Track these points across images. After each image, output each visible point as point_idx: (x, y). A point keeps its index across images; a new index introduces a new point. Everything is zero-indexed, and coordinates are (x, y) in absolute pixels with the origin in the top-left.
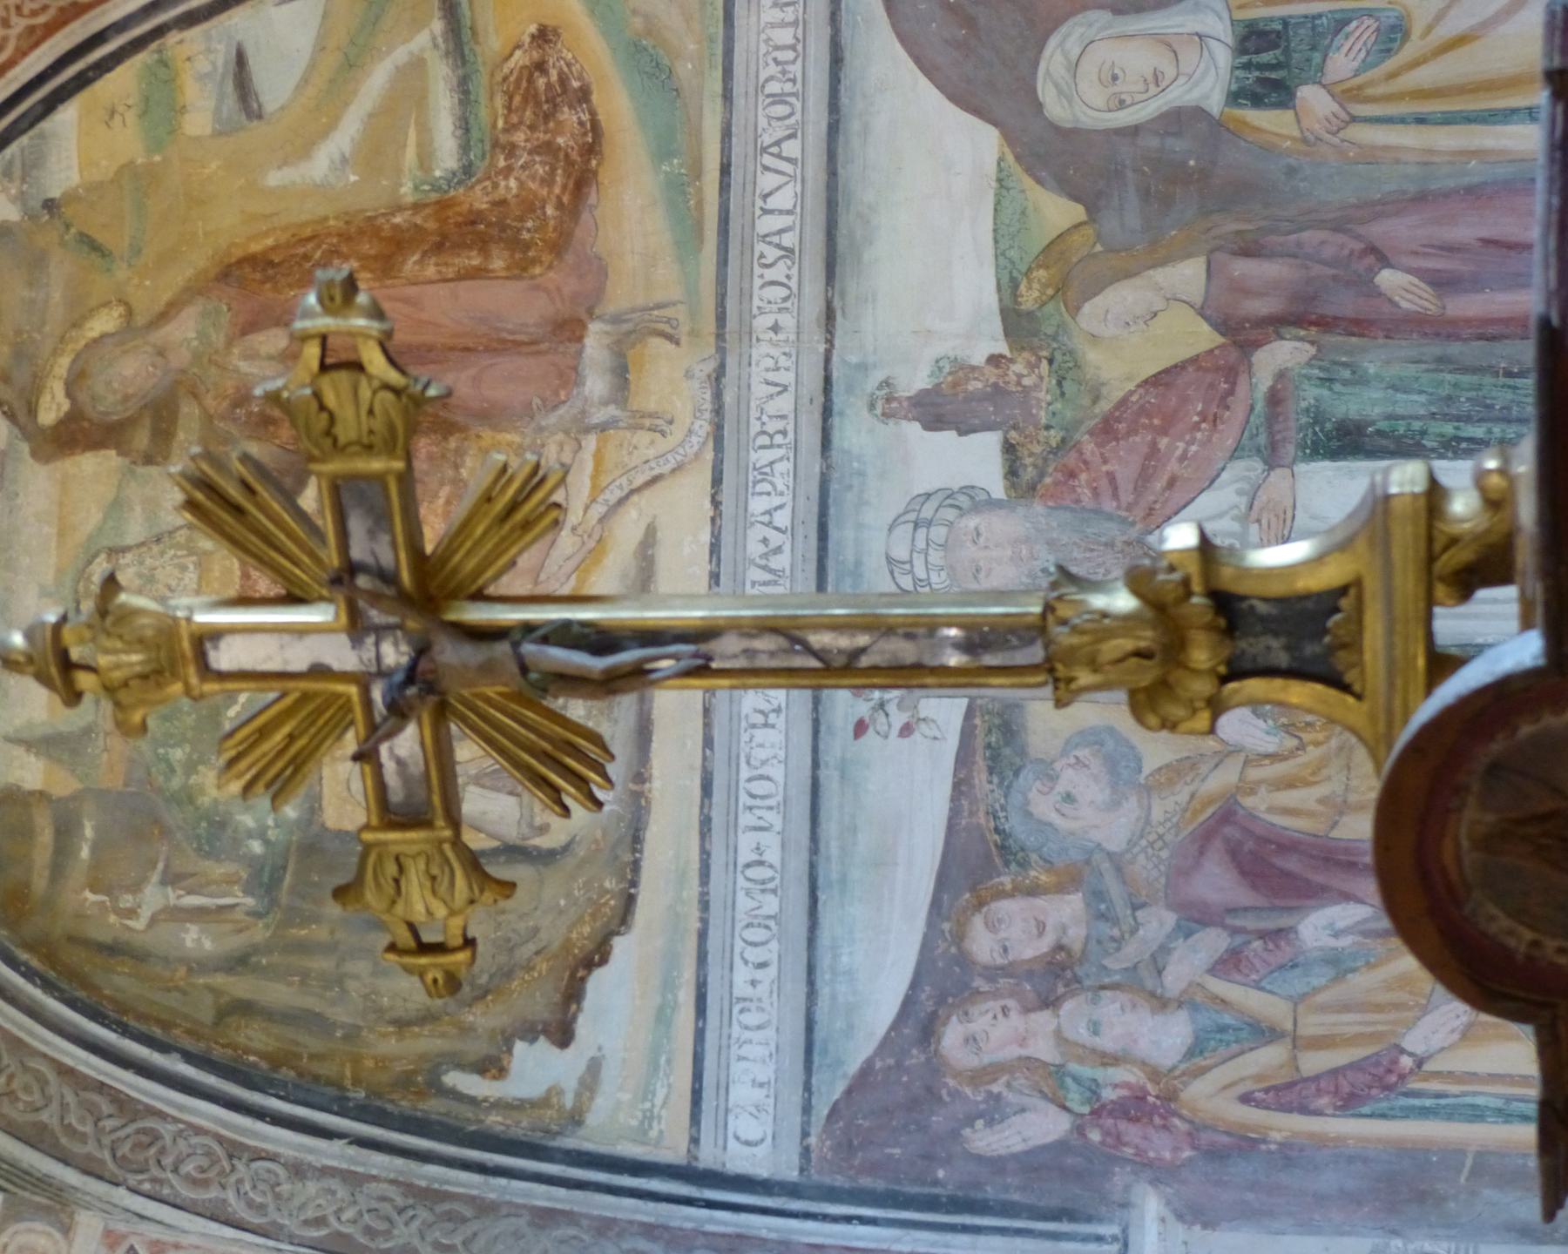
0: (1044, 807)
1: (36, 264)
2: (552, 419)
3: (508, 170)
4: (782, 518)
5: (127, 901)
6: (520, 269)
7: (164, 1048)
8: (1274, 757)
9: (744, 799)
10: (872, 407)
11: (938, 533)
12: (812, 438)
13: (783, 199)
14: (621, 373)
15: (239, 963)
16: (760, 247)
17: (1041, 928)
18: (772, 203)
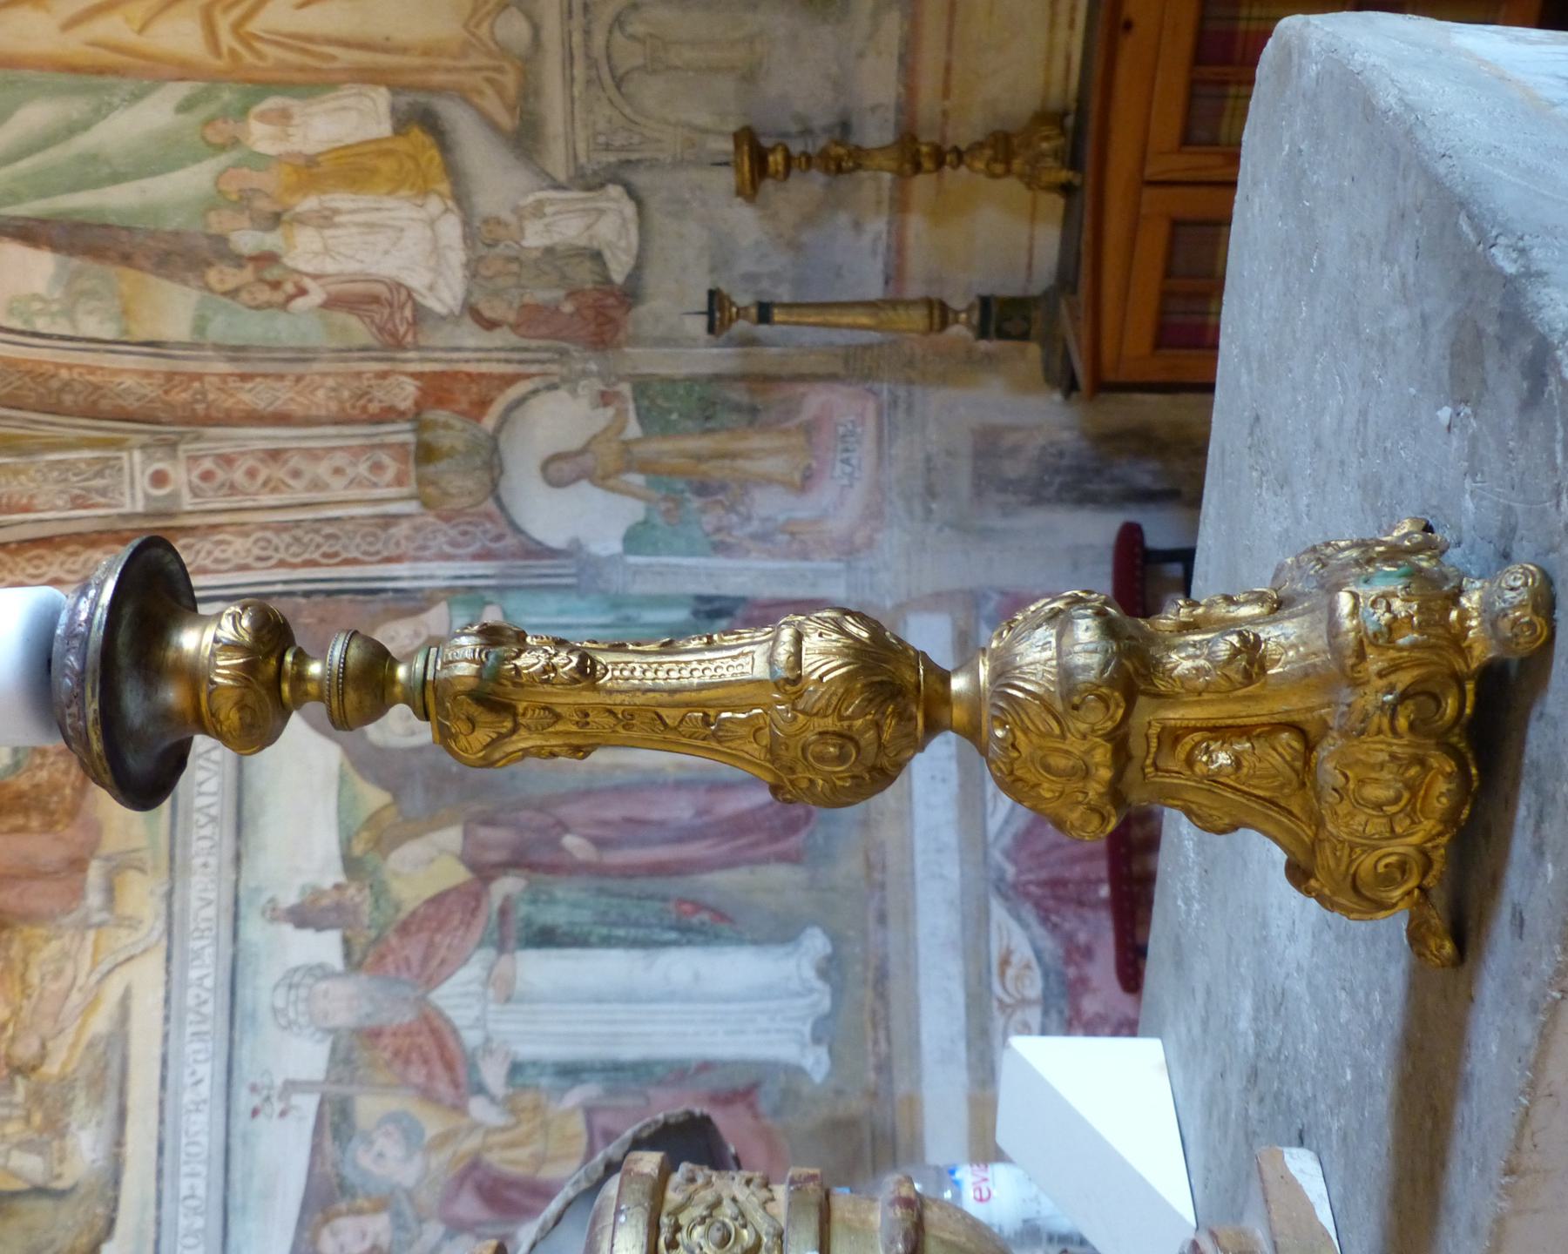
0: (365, 1160)
2: (67, 920)
3: (41, 767)
4: (208, 983)
6: (49, 826)
8: (503, 1129)
9: (183, 1157)
10: (263, 913)
11: (303, 992)
12: (226, 934)
13: (211, 786)
14: (110, 892)
16: (196, 816)
17: (364, 1235)
18: (205, 788)
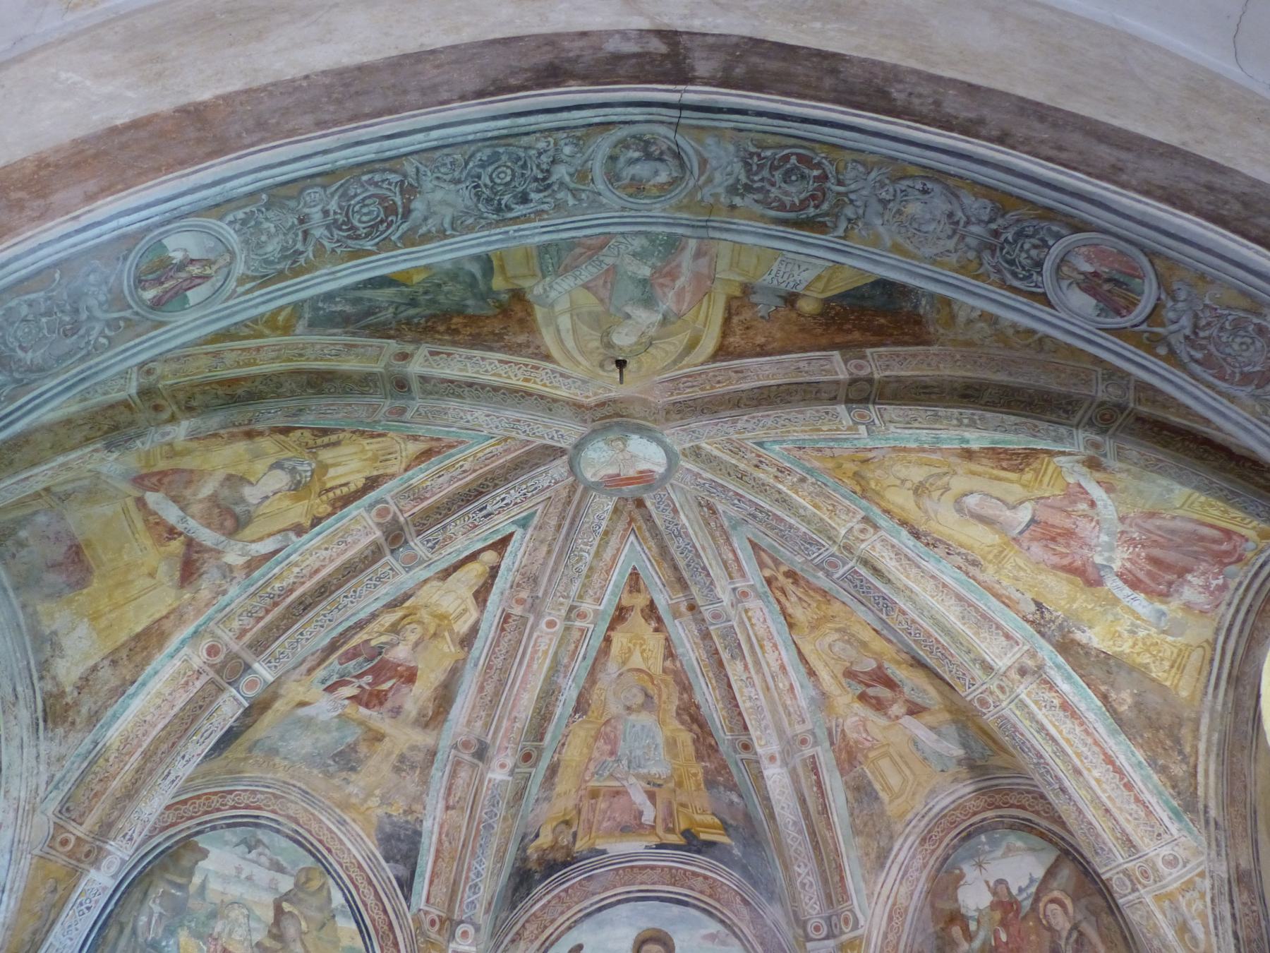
1: (321, 909)
5: (158, 901)
7: (116, 904)
15: (134, 932)
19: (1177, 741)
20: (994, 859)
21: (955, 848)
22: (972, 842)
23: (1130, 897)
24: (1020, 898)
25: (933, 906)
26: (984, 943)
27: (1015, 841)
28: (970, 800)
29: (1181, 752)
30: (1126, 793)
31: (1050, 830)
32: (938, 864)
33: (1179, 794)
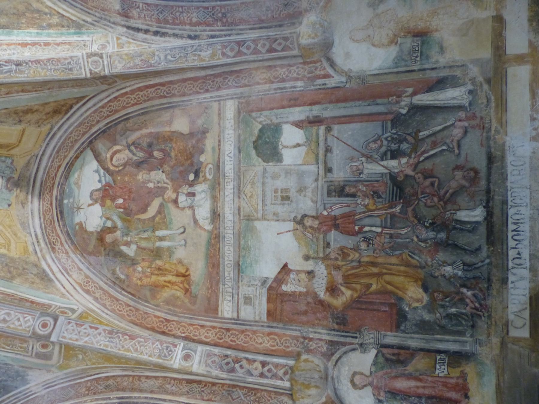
19: (38, 11)
20: (79, 196)
21: (64, 225)
22: (65, 210)
23: (106, 63)
24: (104, 183)
25: (90, 254)
26: (120, 217)
27: (73, 178)
28: (43, 205)
29: (46, 14)
30: (50, 47)
31: (76, 151)
32: (69, 242)
33: (68, 27)
